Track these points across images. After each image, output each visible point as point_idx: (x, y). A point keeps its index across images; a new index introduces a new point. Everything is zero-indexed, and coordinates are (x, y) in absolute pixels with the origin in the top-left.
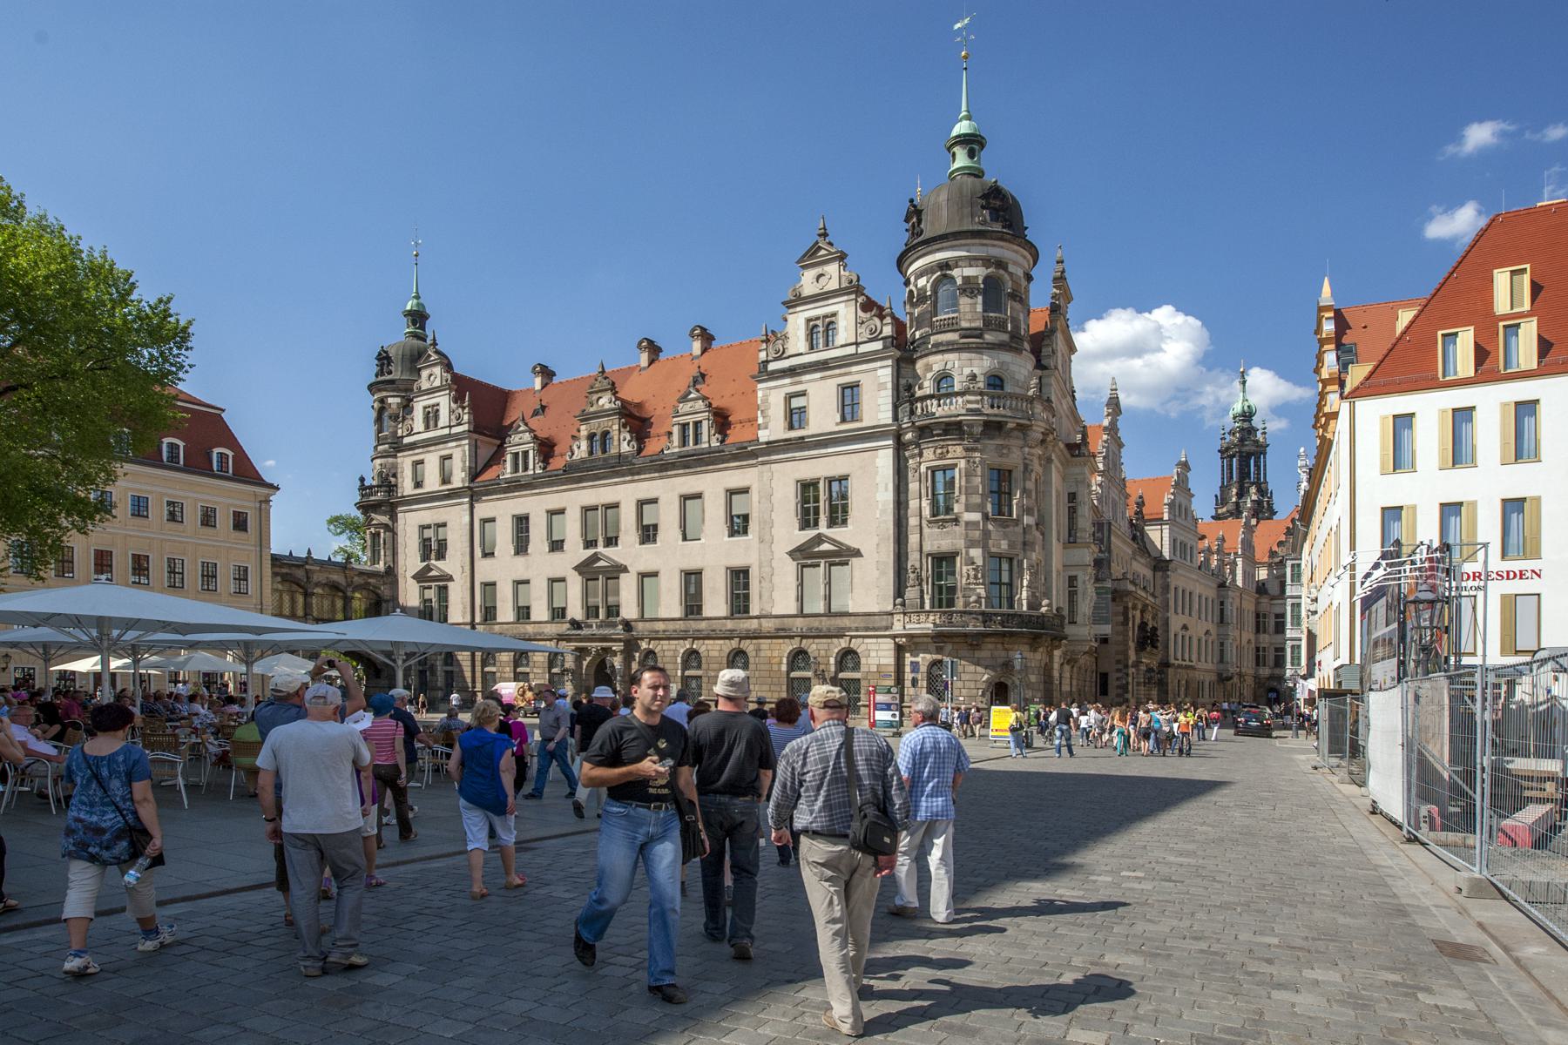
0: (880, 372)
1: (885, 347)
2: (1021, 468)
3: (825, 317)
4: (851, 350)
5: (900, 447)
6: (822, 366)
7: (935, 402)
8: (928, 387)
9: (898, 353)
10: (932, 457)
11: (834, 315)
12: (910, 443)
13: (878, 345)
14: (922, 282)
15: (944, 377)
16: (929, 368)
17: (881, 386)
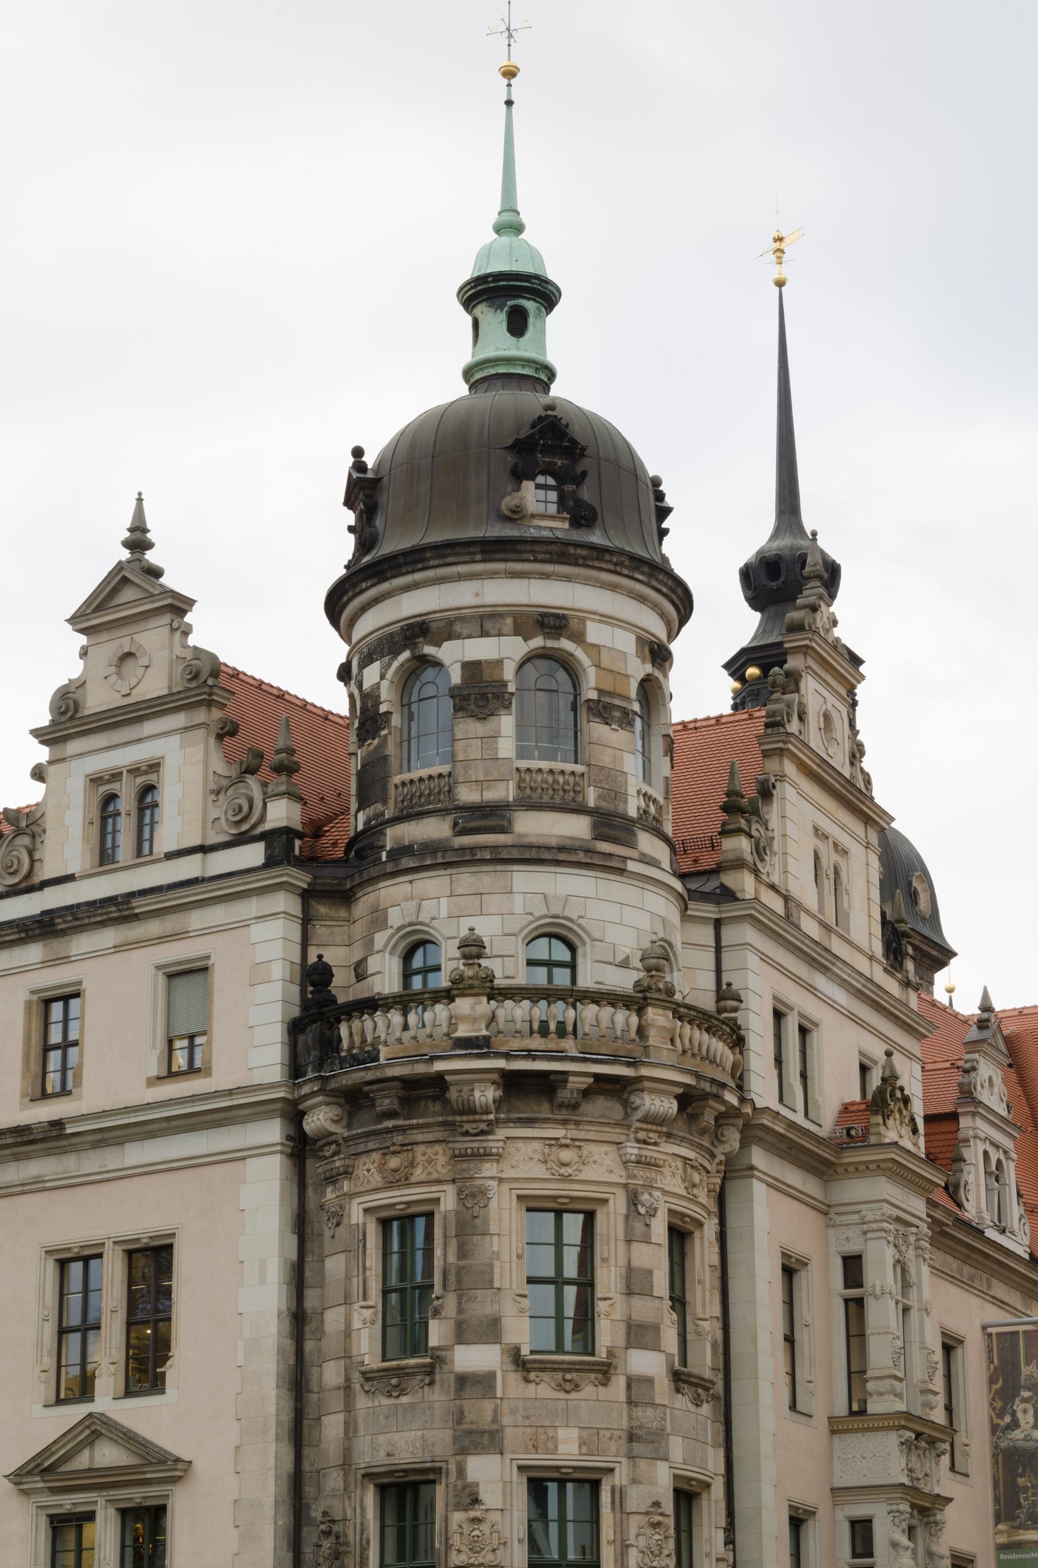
0: (259, 932)
1: (270, 863)
2: (618, 1204)
3: (135, 771)
4: (189, 868)
5: (301, 1148)
6: (116, 911)
7: (396, 1017)
8: (385, 975)
9: (301, 879)
10: (376, 1179)
11: (155, 767)
12: (326, 1136)
13: (253, 854)
14: (371, 675)
15: (415, 945)
16: (378, 919)
17: (257, 974)
